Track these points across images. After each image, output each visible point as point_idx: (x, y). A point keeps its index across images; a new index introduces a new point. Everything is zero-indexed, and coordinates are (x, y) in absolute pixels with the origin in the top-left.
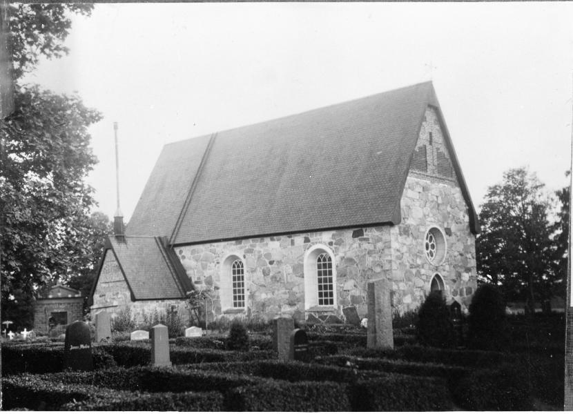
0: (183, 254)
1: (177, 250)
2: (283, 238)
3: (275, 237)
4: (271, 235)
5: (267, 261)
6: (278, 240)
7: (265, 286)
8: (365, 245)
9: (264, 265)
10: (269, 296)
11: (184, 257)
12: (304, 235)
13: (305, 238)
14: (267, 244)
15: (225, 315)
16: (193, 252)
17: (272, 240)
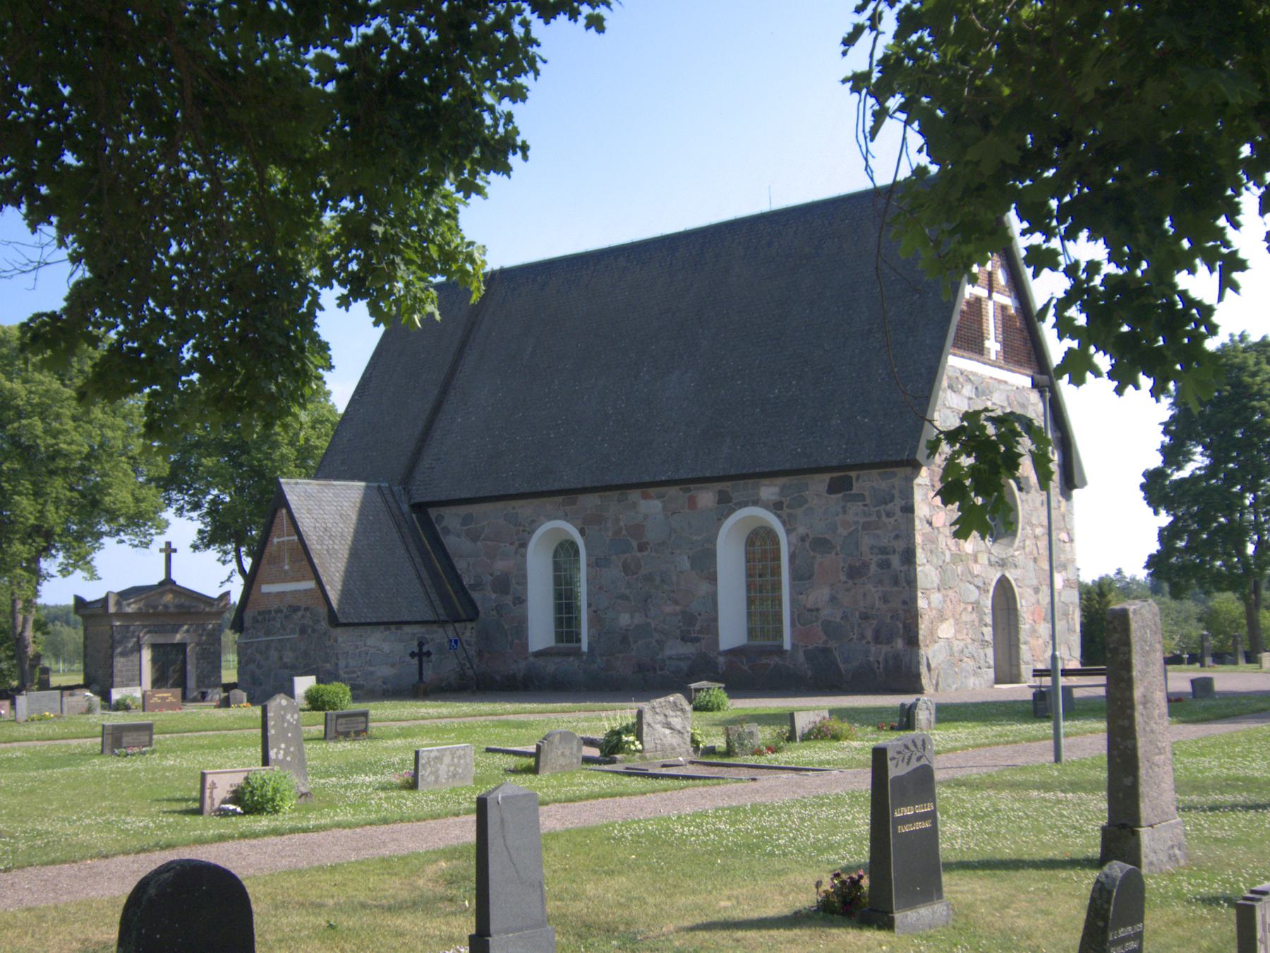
0: (444, 523)
1: (433, 513)
2: (673, 491)
3: (652, 491)
5: (635, 544)
6: (660, 497)
7: (627, 598)
8: (855, 507)
10: (639, 619)
11: (447, 531)
13: (721, 492)
14: (634, 505)
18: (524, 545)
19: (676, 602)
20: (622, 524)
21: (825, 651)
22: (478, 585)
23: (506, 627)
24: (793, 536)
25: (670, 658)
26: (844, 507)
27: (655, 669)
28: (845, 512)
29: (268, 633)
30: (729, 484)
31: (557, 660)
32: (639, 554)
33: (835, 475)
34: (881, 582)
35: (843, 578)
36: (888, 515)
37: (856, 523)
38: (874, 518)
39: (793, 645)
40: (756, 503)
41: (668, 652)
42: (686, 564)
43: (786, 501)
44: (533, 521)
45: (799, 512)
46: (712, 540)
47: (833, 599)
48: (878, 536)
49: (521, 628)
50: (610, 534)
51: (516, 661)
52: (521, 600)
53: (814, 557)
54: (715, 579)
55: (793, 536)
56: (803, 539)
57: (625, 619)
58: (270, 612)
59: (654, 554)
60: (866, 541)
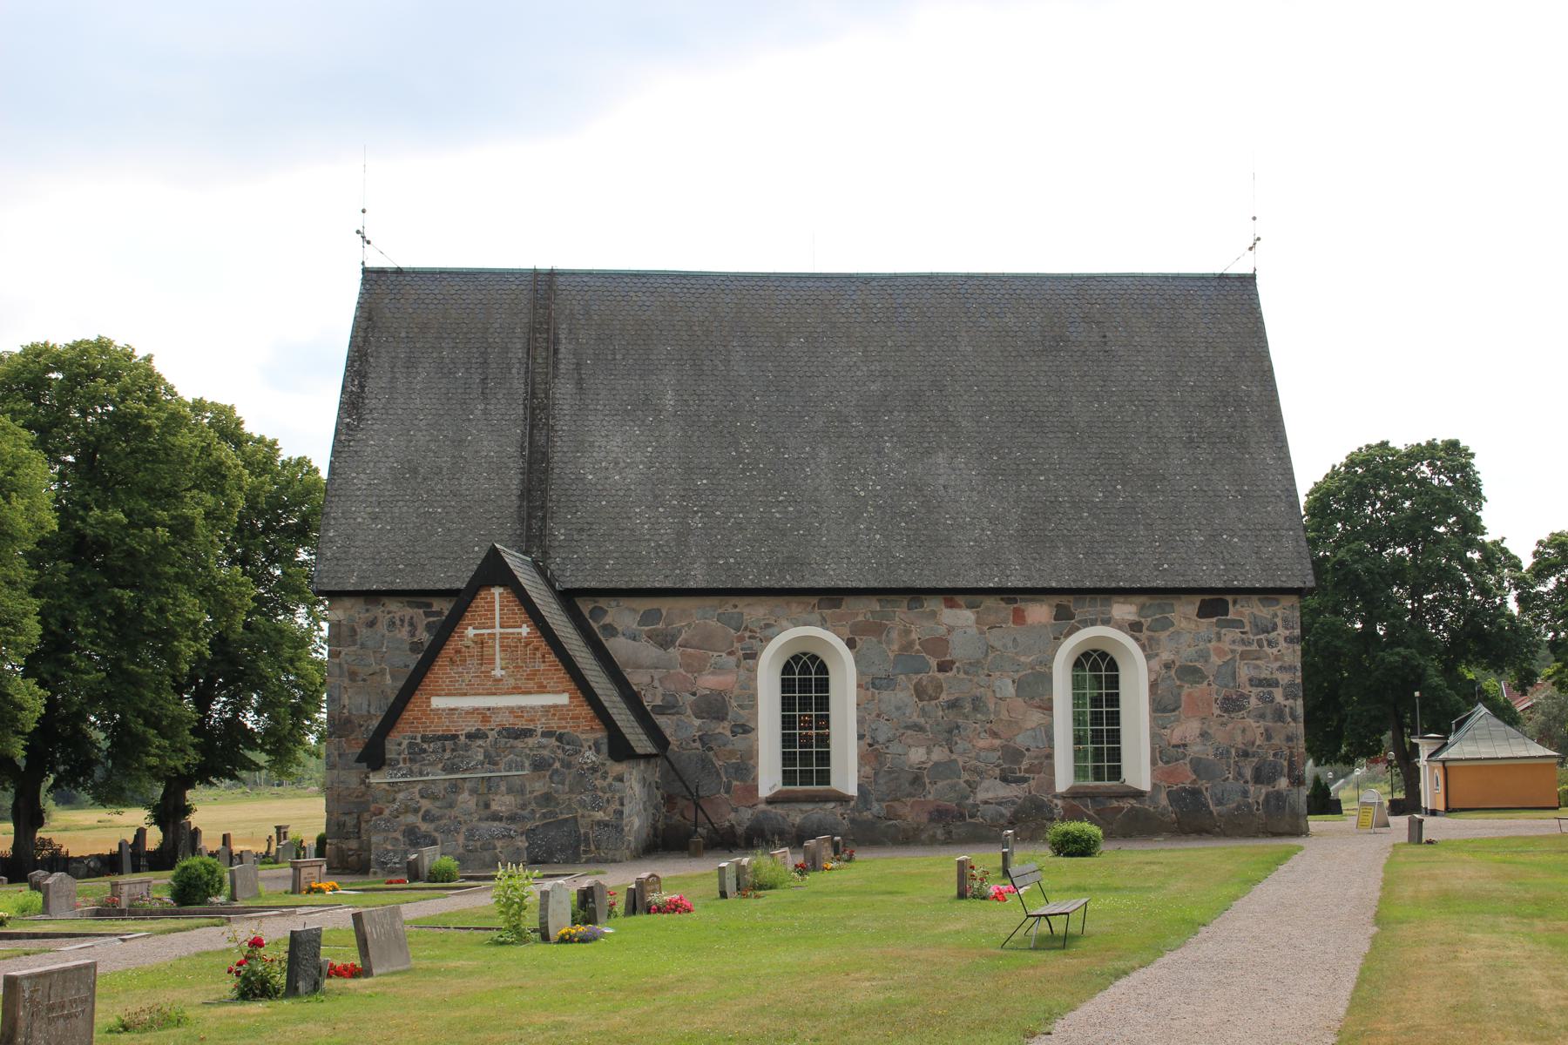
0: (607, 620)
2: (990, 602)
3: (960, 599)
4: (950, 594)
5: (933, 662)
6: (970, 606)
7: (919, 728)
8: (1230, 634)
9: (924, 668)
10: (939, 755)
11: (611, 630)
12: (1056, 600)
14: (933, 614)
15: (779, 810)
16: (649, 617)
17: (951, 605)
18: (753, 656)
19: (995, 735)
20: (914, 636)
21: (1195, 793)
22: (668, 707)
23: (718, 763)
24: (1155, 663)
25: (986, 803)
26: (1218, 634)
27: (962, 816)
28: (1219, 639)
29: (450, 768)
30: (1071, 598)
31: (808, 807)
32: (940, 676)
33: (1207, 597)
34: (1262, 716)
35: (1218, 712)
36: (1270, 644)
37: (1233, 651)
38: (1255, 647)
39: (1154, 786)
40: (1106, 622)
41: (982, 796)
42: (1010, 690)
43: (1146, 622)
44: (768, 626)
45: (1163, 635)
46: (1048, 663)
47: (1204, 735)
48: (1257, 667)
49: (745, 768)
50: (896, 647)
51: (736, 810)
52: (746, 729)
53: (1180, 687)
54: (1051, 709)
55: (1155, 663)
56: (1167, 666)
57: (917, 755)
58: (455, 737)
59: (961, 675)
60: (1244, 672)
